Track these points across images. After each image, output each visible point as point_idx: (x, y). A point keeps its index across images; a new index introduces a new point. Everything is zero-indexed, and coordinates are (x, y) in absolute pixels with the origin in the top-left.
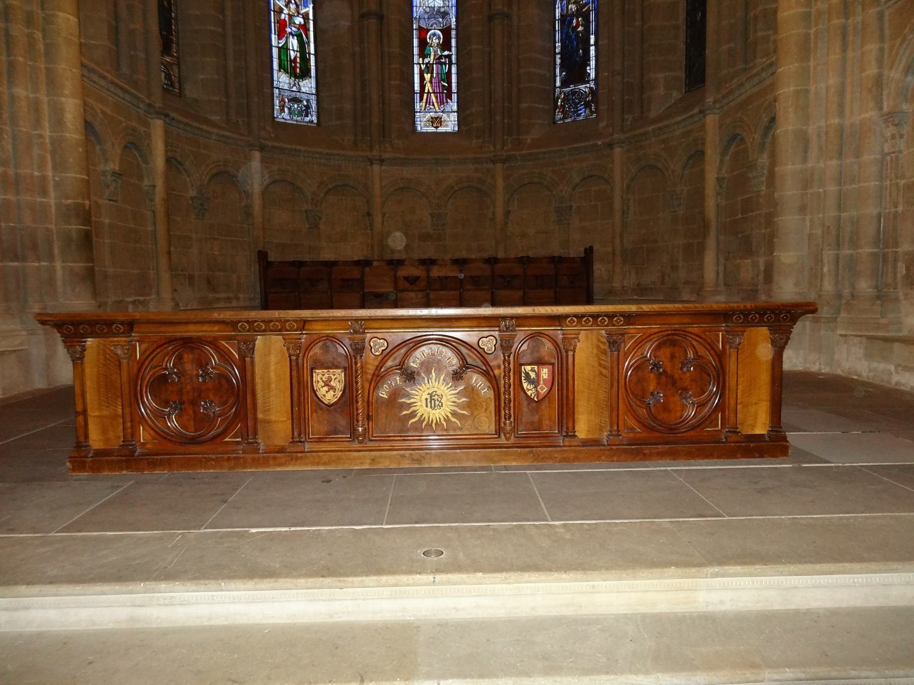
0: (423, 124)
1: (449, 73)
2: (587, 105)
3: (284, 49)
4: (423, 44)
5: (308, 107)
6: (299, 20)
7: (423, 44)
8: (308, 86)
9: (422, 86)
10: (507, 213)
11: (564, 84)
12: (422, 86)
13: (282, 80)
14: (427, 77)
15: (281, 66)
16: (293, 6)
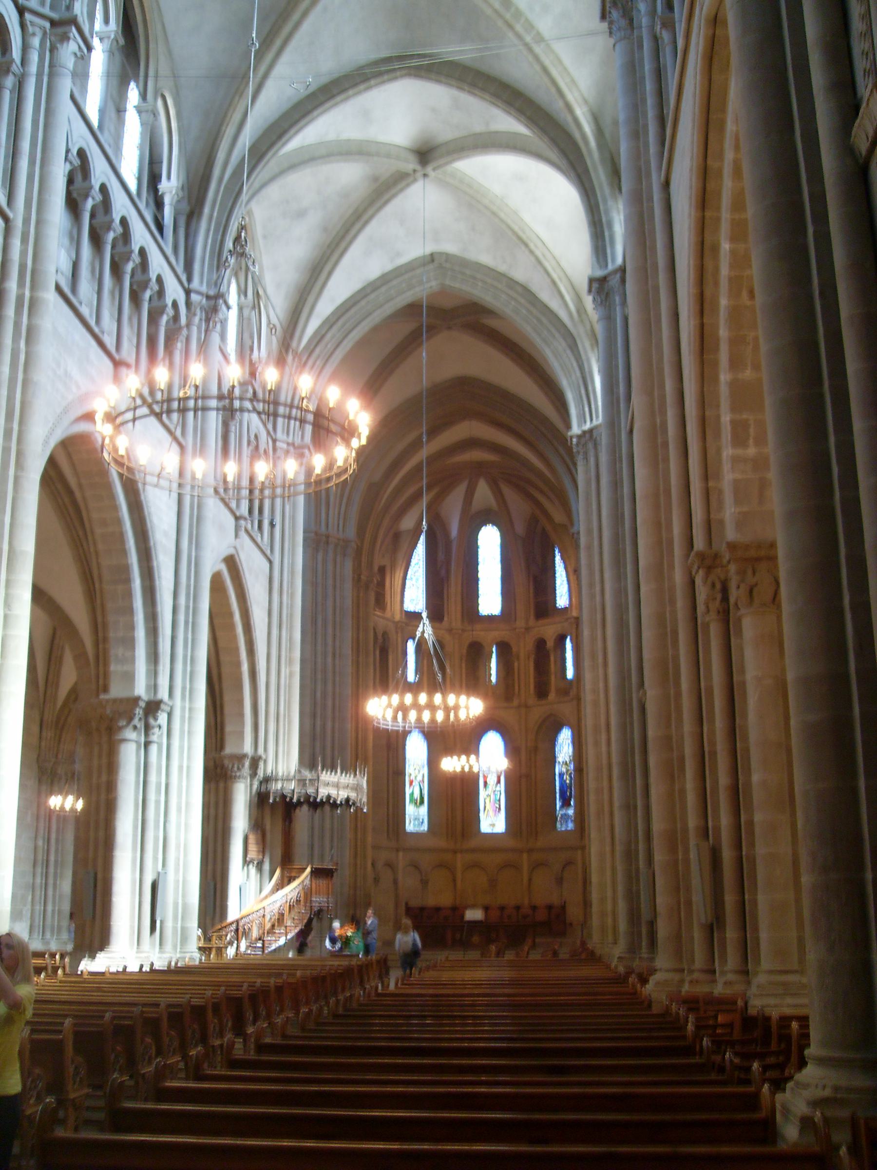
0: (486, 827)
1: (499, 800)
2: (572, 821)
3: (412, 794)
4: (486, 784)
5: (422, 823)
6: (420, 778)
7: (486, 784)
8: (424, 810)
9: (485, 807)
10: (530, 880)
11: (562, 807)
12: (485, 807)
13: (410, 809)
14: (487, 801)
15: (411, 801)
16: (417, 771)
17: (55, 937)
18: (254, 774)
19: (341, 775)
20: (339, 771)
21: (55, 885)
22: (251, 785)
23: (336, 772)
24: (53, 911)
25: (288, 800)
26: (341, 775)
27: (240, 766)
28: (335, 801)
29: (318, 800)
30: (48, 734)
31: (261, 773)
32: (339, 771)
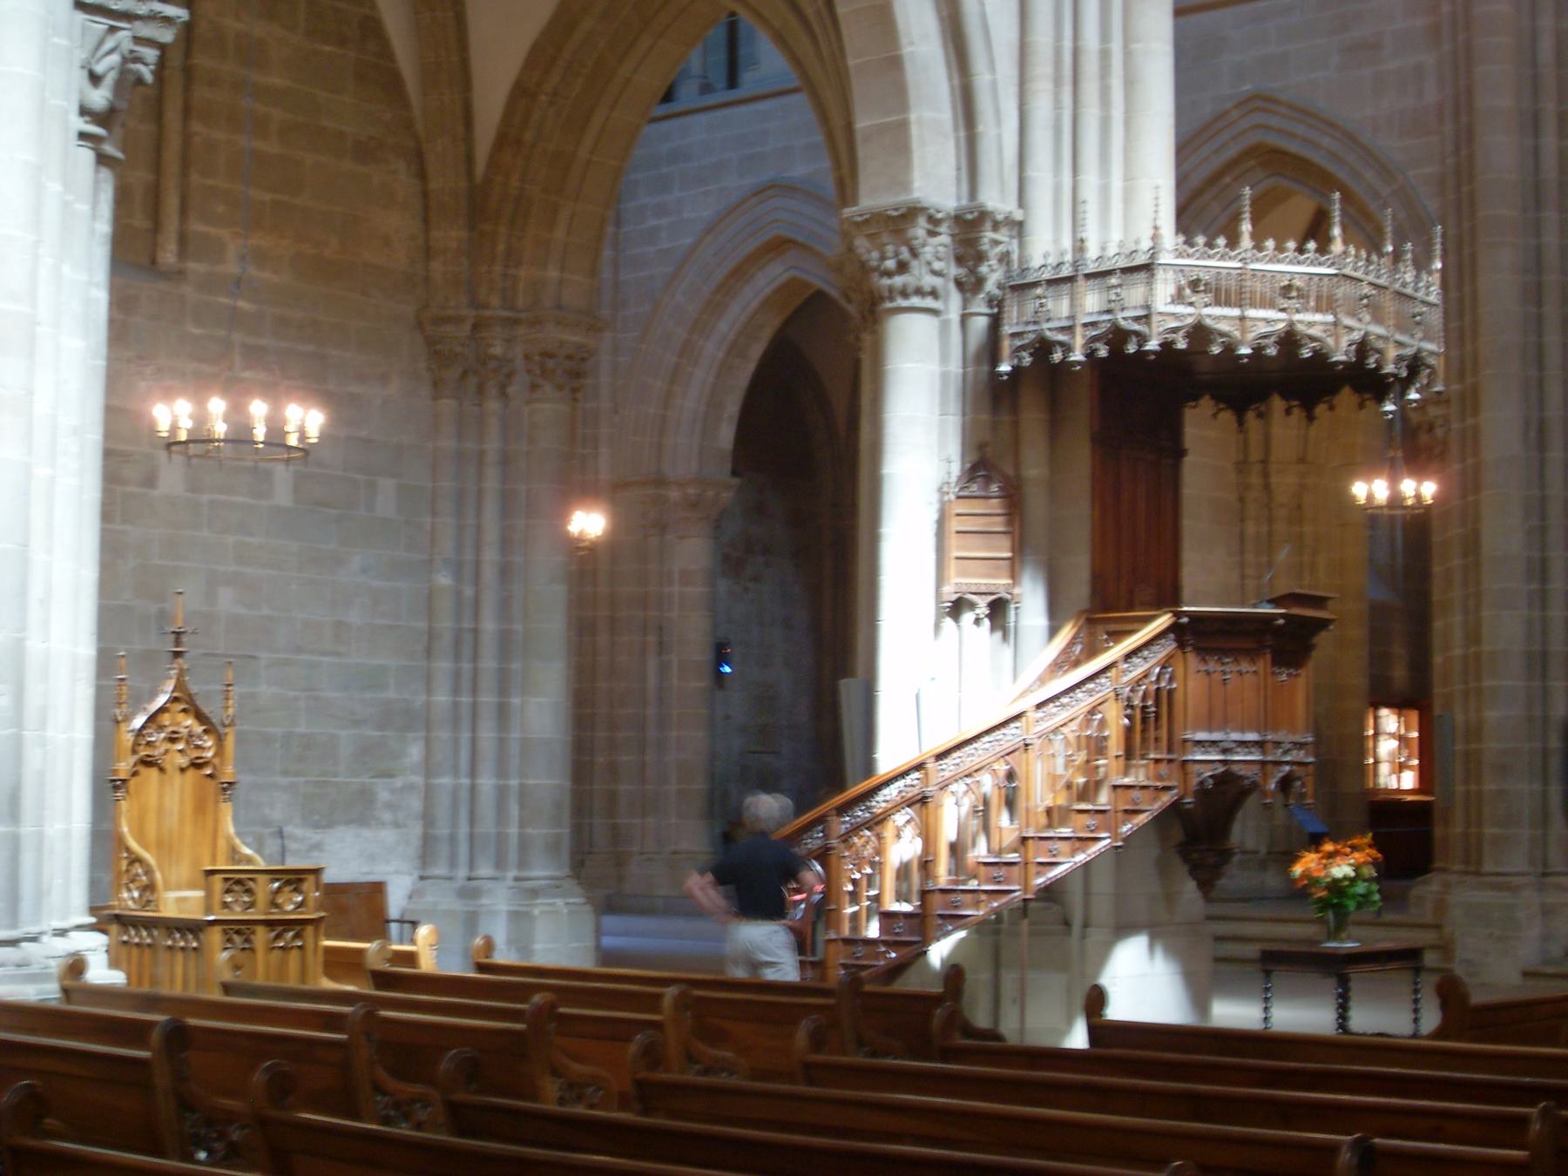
17: (512, 873)
18: (969, 286)
19: (1259, 247)
20: (1246, 227)
21: (503, 712)
22: (964, 319)
23: (1233, 242)
24: (502, 793)
25: (1057, 356)
26: (1259, 247)
27: (905, 254)
28: (1230, 349)
29: (1153, 345)
30: (451, 235)
31: (993, 276)
32: (1246, 227)
